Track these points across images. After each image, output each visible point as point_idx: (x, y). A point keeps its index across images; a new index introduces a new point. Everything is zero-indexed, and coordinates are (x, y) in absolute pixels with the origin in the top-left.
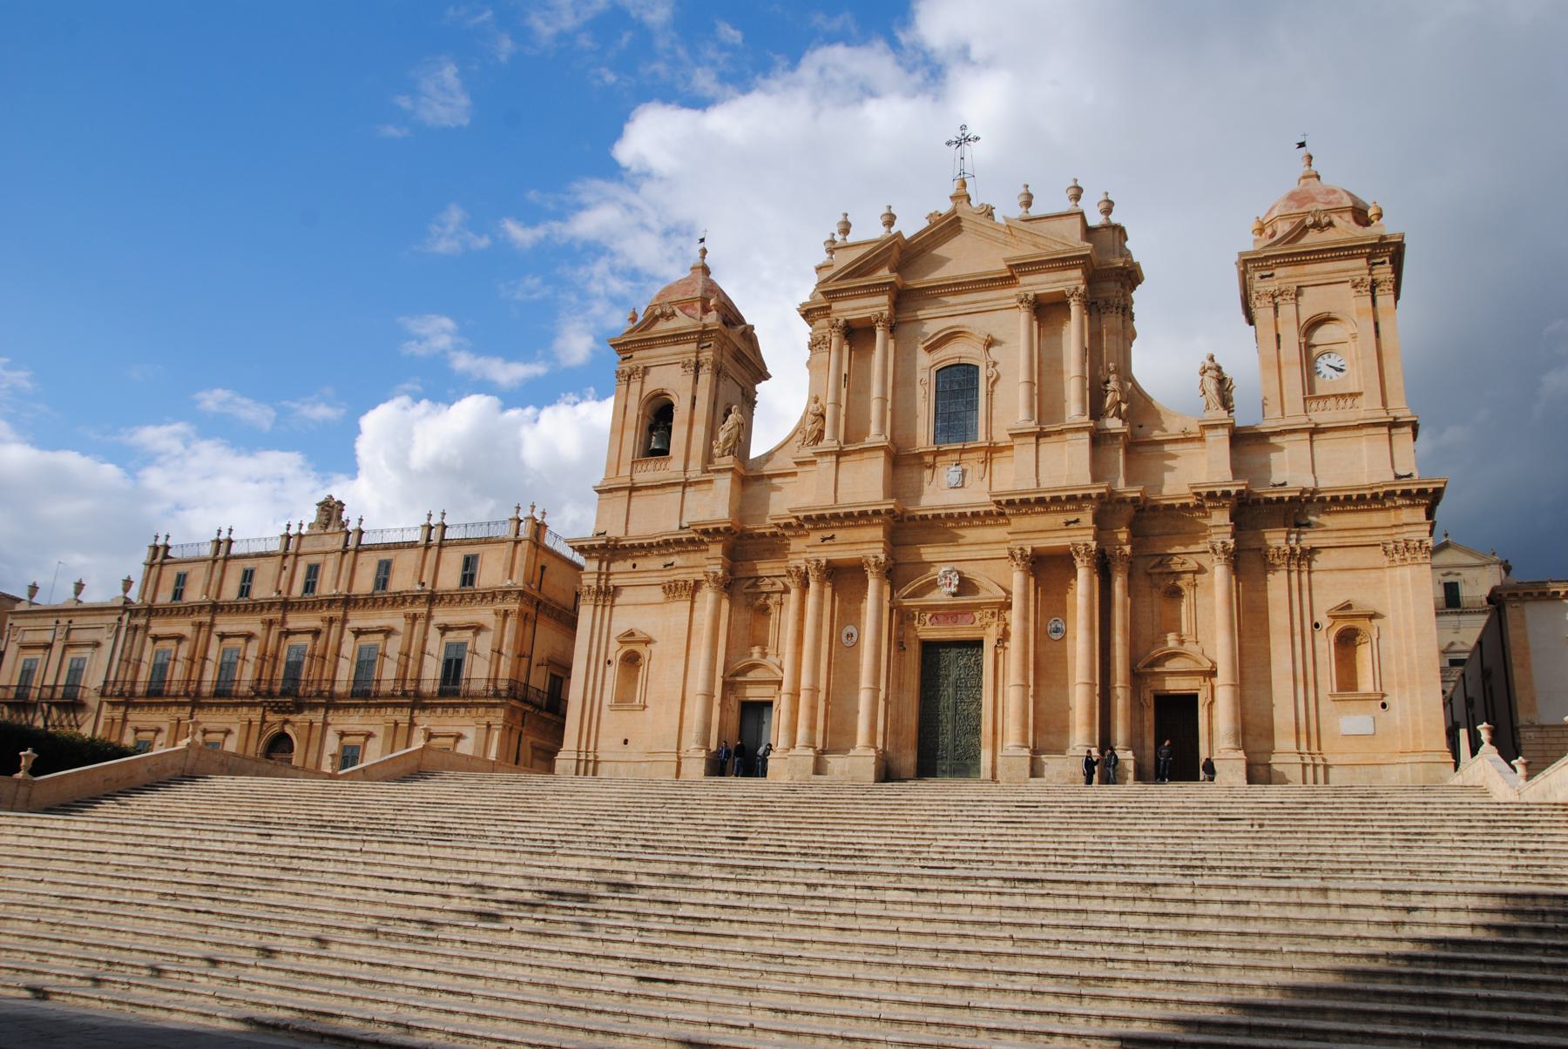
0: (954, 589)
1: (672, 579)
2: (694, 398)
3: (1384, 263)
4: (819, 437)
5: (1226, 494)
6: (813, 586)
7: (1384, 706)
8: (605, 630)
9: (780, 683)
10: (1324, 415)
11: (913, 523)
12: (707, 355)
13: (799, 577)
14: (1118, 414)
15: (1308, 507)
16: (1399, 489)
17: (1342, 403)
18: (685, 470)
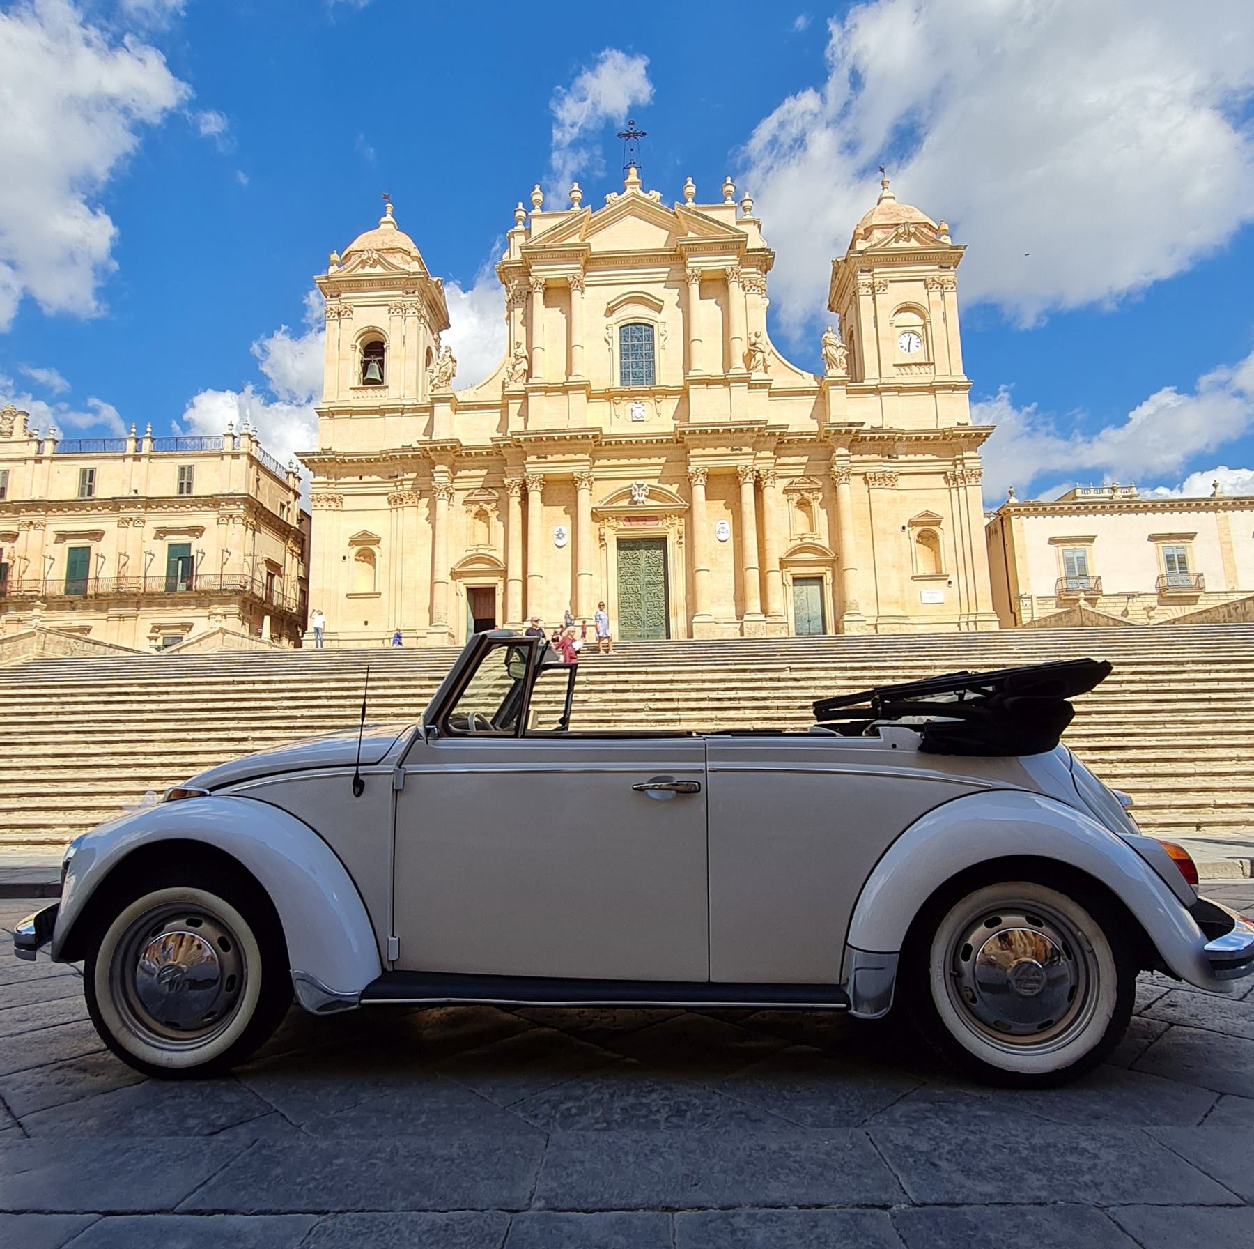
0: (643, 498)
3: (949, 268)
4: (528, 373)
9: (506, 571)
11: (608, 447)
12: (413, 299)
15: (898, 443)
16: (963, 433)
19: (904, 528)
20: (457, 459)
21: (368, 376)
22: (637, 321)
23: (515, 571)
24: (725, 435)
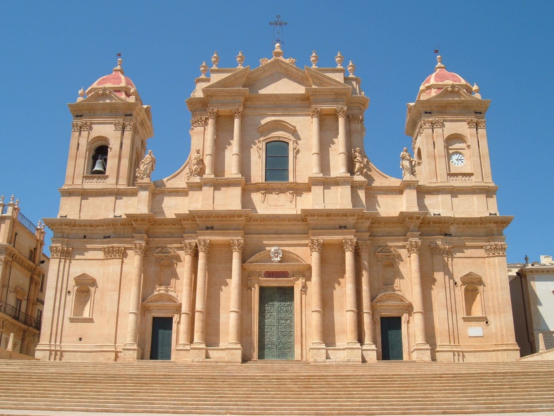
0: (279, 259)
1: (110, 245)
2: (121, 144)
5: (418, 218)
6: (201, 255)
7: (487, 323)
8: (66, 273)
9: (181, 306)
10: (458, 183)
11: (255, 223)
13: (190, 248)
14: (361, 174)
17: (464, 178)
18: (117, 183)
19: (456, 284)
20: (152, 227)
22: (277, 139)
24: (335, 218)
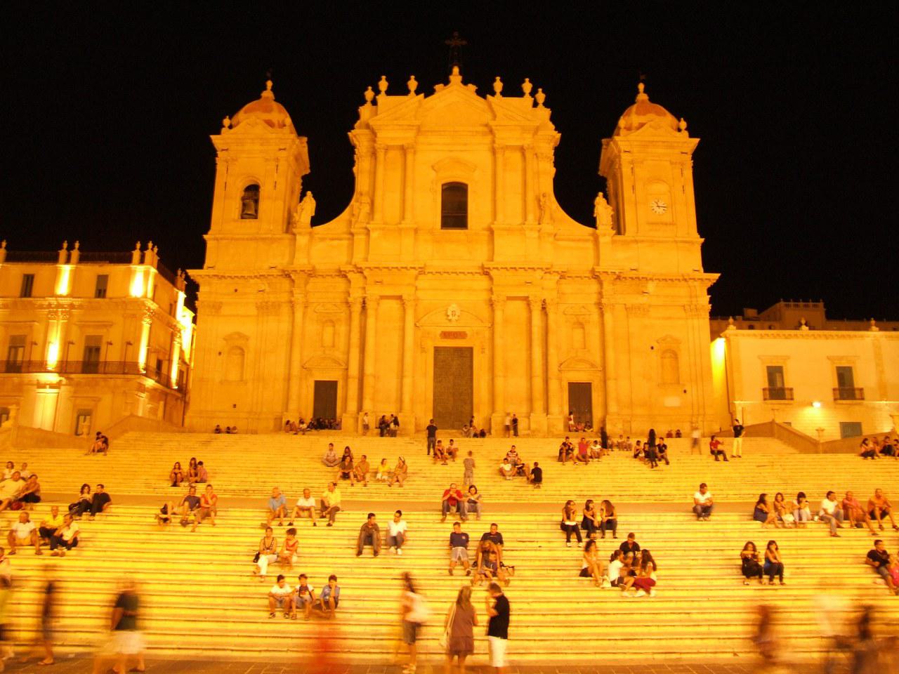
0: (456, 318)
19: (652, 348)
21: (246, 212)
23: (354, 370)
